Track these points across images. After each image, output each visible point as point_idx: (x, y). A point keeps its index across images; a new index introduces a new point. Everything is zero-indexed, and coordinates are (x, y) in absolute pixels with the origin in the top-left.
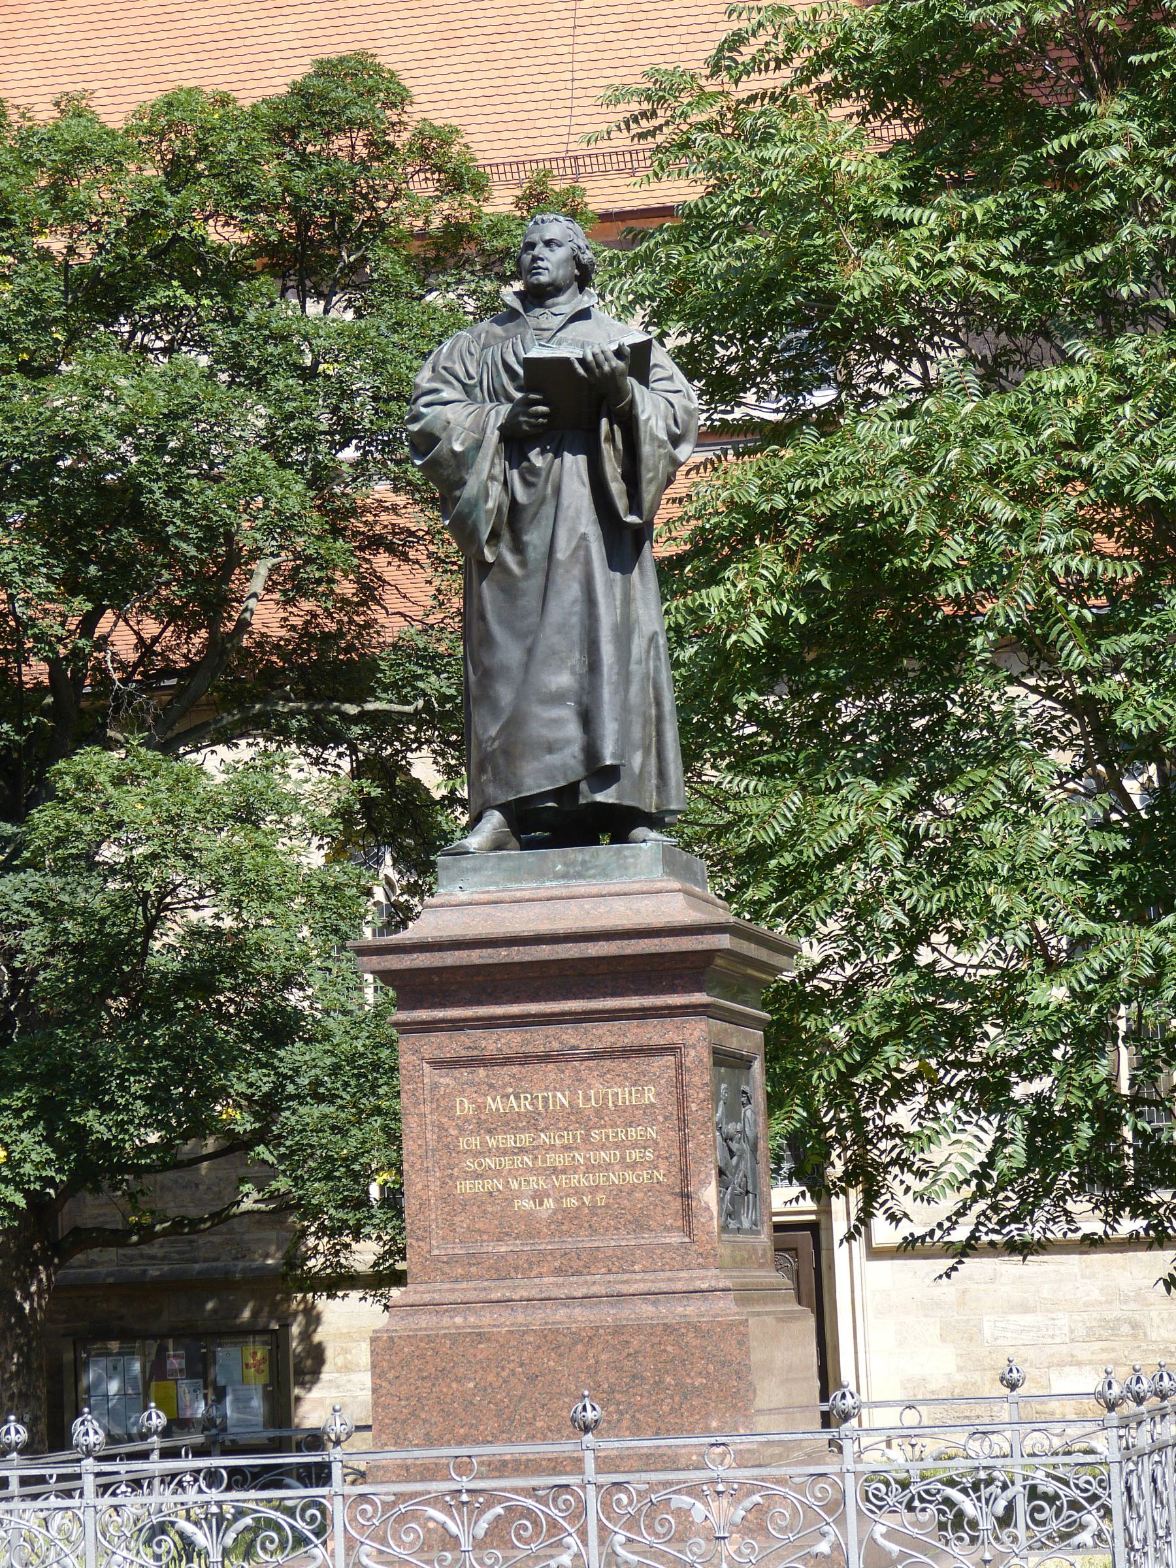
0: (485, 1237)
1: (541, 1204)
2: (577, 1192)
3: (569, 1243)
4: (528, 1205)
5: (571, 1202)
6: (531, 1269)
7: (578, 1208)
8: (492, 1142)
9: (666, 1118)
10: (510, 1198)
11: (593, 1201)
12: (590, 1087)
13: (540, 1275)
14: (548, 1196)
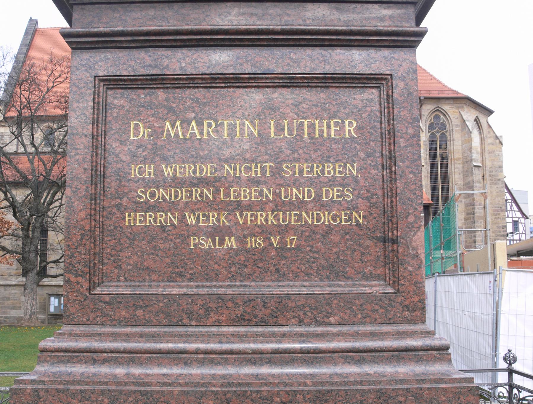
0: (154, 277)
1: (222, 243)
2: (265, 232)
3: (251, 288)
4: (206, 244)
5: (256, 242)
6: (207, 316)
7: (264, 249)
8: (168, 172)
9: (368, 155)
10: (185, 233)
11: (282, 242)
12: (283, 116)
13: (218, 324)
14: (230, 235)
